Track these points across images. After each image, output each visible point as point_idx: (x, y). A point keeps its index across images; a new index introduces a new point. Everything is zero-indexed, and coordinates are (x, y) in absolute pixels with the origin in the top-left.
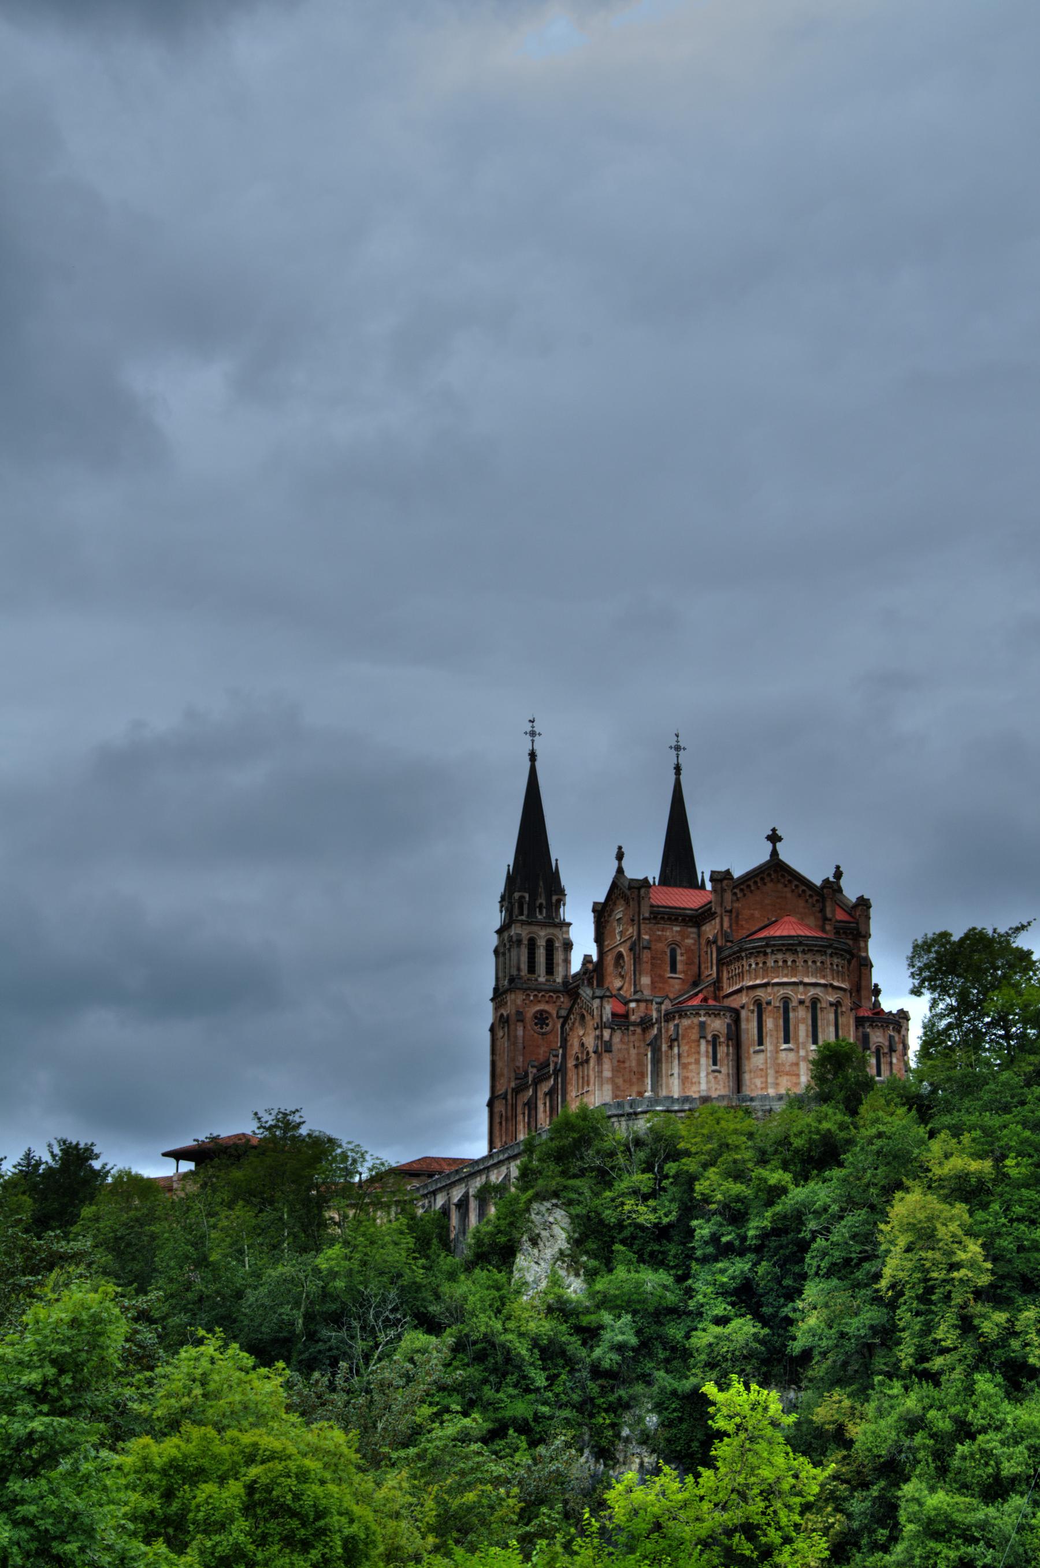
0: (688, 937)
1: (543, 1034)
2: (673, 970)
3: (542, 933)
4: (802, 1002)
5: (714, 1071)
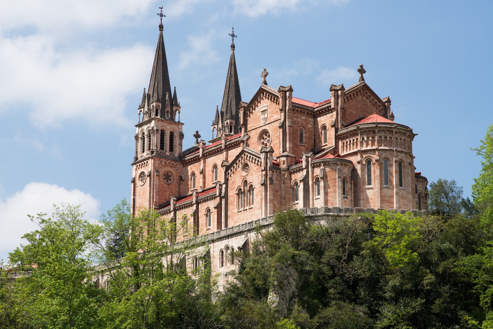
0: (309, 124)
1: (169, 184)
2: (301, 141)
3: (168, 127)
5: (344, 197)
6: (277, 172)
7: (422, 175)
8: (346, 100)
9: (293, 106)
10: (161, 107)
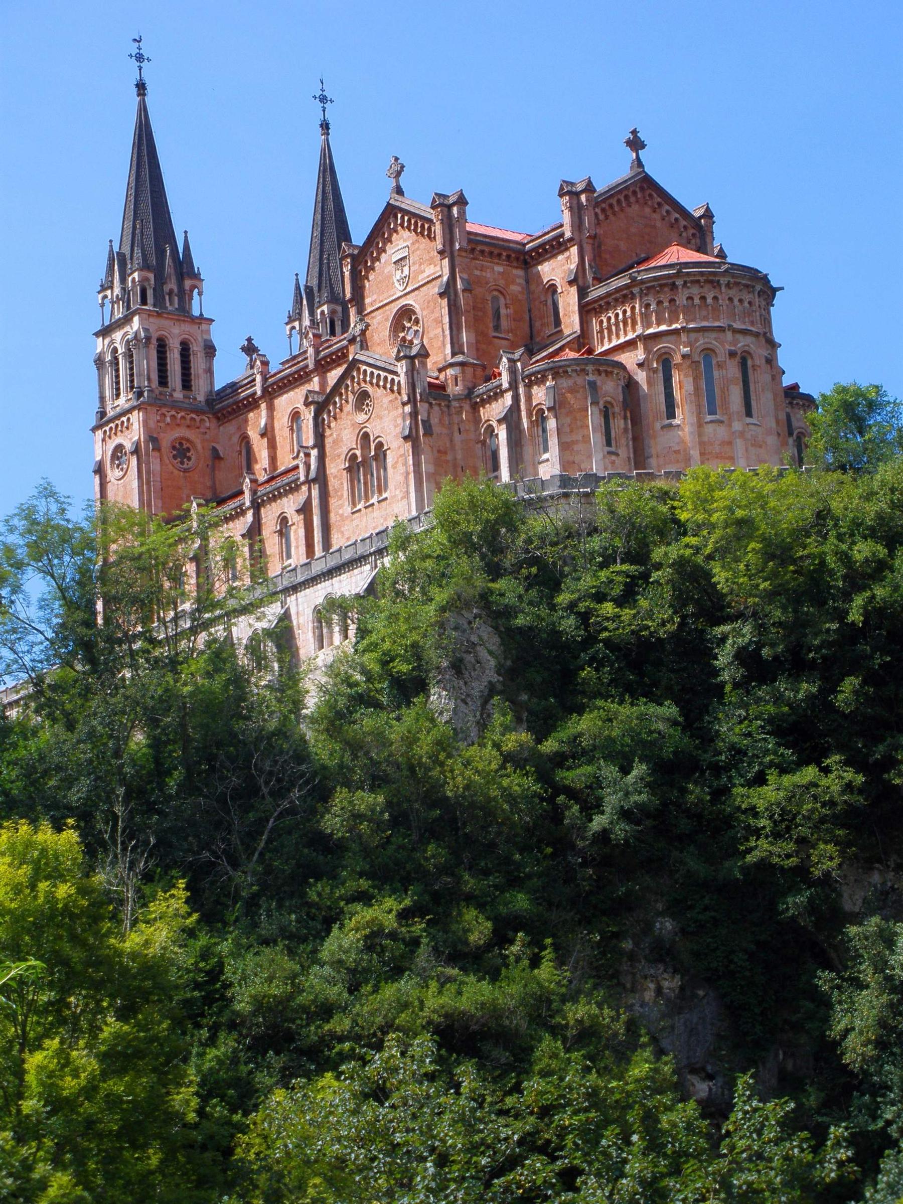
0: (513, 282)
1: (185, 471)
2: (497, 328)
3: (176, 330)
4: (732, 354)
5: (609, 453)
6: (440, 405)
7: (801, 391)
8: (601, 217)
9: (470, 241)
10: (153, 282)
